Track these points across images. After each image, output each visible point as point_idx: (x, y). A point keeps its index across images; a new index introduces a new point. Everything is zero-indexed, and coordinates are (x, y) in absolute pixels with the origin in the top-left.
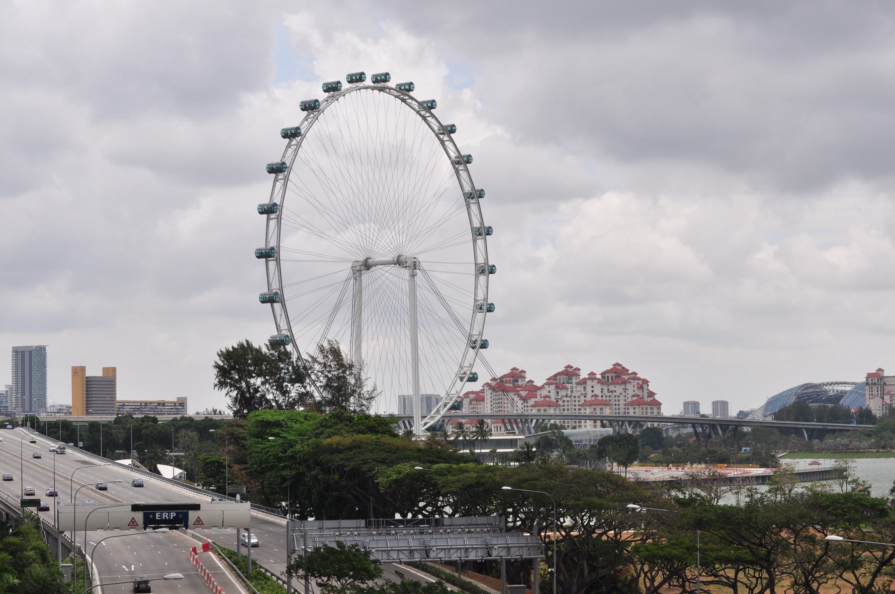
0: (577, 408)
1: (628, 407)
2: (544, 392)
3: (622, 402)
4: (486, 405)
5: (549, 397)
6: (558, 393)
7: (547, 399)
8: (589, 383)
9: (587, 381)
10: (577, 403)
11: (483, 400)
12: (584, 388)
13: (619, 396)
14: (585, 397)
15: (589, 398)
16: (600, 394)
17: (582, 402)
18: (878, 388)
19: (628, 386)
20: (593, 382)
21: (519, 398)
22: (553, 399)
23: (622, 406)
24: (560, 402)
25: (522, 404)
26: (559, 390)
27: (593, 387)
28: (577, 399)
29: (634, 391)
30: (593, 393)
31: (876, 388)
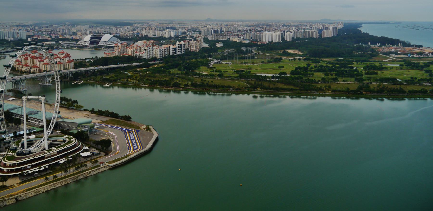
2: (46, 61)
3: (65, 62)
5: (47, 62)
11: (28, 60)
16: (60, 61)
19: (66, 58)
22: (48, 63)
23: (65, 63)
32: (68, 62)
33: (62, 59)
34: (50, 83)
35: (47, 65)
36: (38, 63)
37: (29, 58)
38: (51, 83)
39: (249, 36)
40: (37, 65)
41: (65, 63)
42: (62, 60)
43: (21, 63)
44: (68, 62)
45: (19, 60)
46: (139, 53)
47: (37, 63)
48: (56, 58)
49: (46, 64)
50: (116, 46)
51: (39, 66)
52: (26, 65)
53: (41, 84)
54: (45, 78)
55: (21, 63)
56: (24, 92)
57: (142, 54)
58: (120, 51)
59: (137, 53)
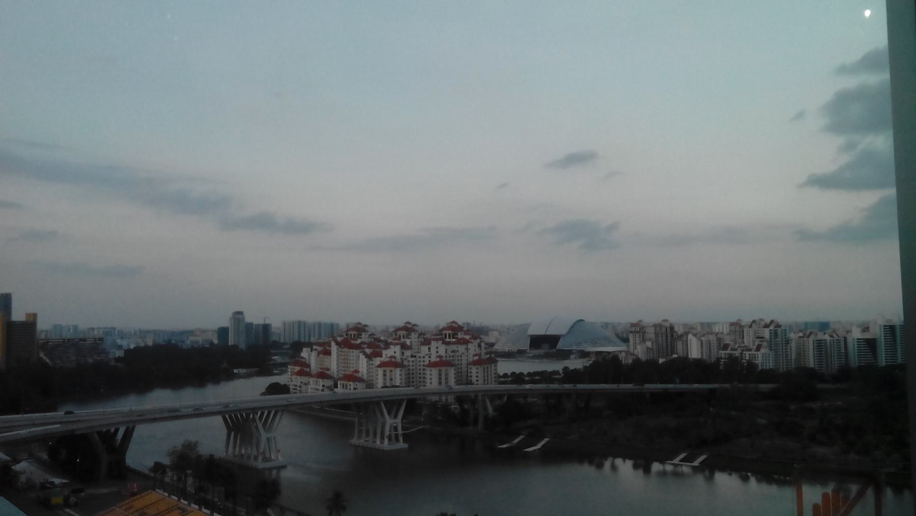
0: (422, 368)
1: (471, 366)
4: (332, 360)
5: (395, 357)
6: (403, 353)
7: (393, 359)
8: (434, 344)
9: (432, 342)
10: (422, 364)
12: (429, 348)
13: (461, 356)
14: (430, 357)
15: (434, 359)
17: (427, 363)
18: (640, 335)
19: (470, 346)
20: (437, 343)
21: (364, 356)
22: (399, 360)
23: (464, 366)
24: (405, 363)
25: (367, 362)
26: (405, 351)
27: (437, 348)
28: (422, 359)
29: (475, 350)
30: (438, 354)
31: (638, 335)
32: (475, 363)
33: (454, 347)
34: (397, 440)
35: (393, 369)
36: (362, 365)
37: (334, 348)
38: (401, 439)
40: (357, 371)
41: (464, 366)
42: (453, 352)
43: (308, 370)
44: (475, 363)
45: (304, 360)
47: (361, 366)
48: (429, 343)
49: (392, 364)
50: (638, 332)
51: (365, 377)
52: (322, 375)
53: (362, 442)
54: (378, 414)
55: (308, 370)
56: (274, 472)
57: (752, 352)
58: (652, 349)
59: (728, 352)
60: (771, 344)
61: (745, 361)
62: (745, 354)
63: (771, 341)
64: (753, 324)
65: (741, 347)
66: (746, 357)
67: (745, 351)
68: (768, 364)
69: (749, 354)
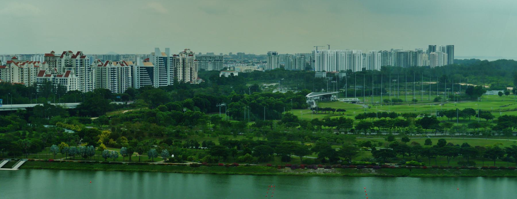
39: (276, 62)
46: (52, 77)
57: (63, 78)
59: (44, 77)
60: (77, 71)
61: (57, 85)
62: (57, 79)
63: (77, 69)
64: (64, 56)
65: (53, 74)
66: (57, 82)
67: (57, 77)
68: (74, 87)
69: (60, 79)
